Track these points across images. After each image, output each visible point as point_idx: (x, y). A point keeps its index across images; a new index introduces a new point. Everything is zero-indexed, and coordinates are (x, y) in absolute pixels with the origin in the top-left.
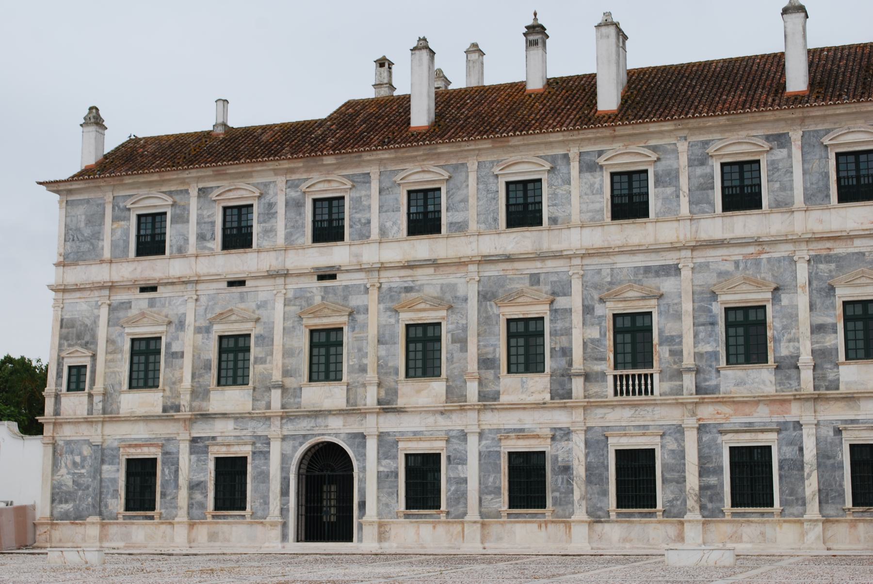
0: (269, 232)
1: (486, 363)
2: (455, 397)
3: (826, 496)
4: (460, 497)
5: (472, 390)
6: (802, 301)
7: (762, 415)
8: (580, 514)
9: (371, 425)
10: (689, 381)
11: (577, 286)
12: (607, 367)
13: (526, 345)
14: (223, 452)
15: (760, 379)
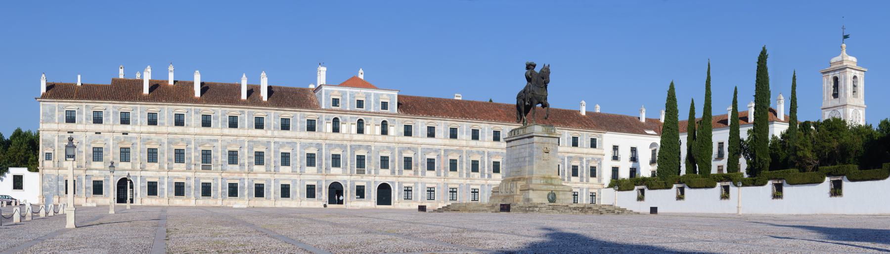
0: (108, 120)
1: (169, 160)
2: (161, 168)
3: (249, 194)
4: (162, 193)
5: (166, 166)
6: (246, 151)
7: (236, 176)
8: (193, 197)
9: (138, 173)
10: (220, 167)
11: (193, 142)
12: (200, 163)
13: (180, 156)
14: (96, 179)
15: (236, 167)
